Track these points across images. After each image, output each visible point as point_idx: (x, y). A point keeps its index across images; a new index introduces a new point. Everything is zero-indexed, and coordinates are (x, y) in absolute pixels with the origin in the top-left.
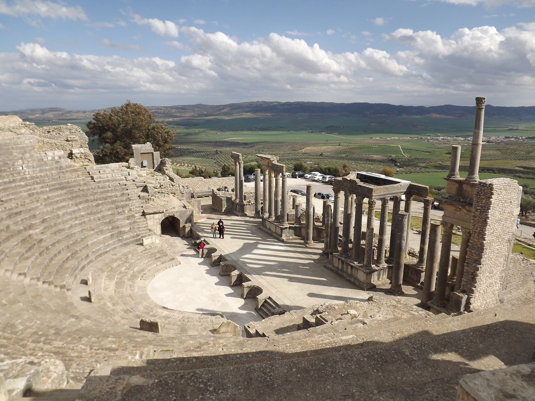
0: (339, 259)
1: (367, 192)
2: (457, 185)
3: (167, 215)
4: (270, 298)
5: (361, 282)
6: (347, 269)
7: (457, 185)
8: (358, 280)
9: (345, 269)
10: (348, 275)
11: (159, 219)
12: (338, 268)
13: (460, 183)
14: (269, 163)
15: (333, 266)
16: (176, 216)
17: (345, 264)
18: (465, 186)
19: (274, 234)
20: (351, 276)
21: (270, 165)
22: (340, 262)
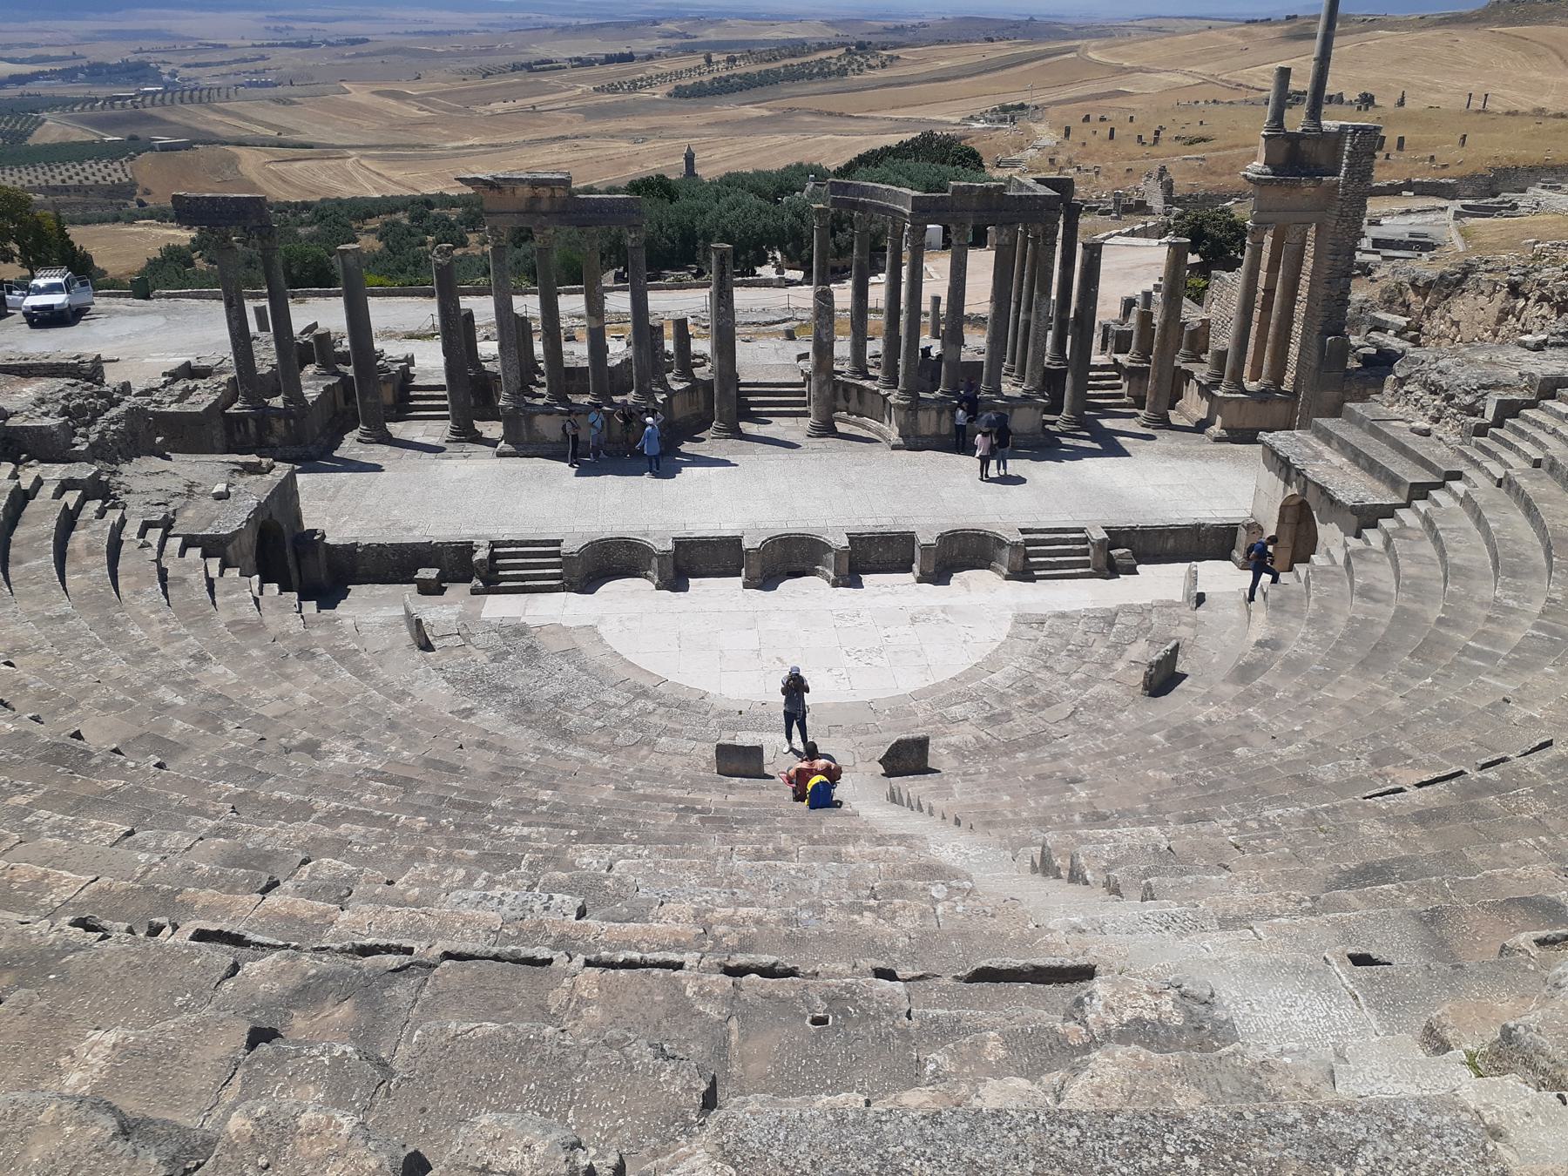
2: (1288, 145)
7: (1288, 145)
12: (938, 435)
13: (1294, 139)
14: (535, 199)
18: (1303, 145)
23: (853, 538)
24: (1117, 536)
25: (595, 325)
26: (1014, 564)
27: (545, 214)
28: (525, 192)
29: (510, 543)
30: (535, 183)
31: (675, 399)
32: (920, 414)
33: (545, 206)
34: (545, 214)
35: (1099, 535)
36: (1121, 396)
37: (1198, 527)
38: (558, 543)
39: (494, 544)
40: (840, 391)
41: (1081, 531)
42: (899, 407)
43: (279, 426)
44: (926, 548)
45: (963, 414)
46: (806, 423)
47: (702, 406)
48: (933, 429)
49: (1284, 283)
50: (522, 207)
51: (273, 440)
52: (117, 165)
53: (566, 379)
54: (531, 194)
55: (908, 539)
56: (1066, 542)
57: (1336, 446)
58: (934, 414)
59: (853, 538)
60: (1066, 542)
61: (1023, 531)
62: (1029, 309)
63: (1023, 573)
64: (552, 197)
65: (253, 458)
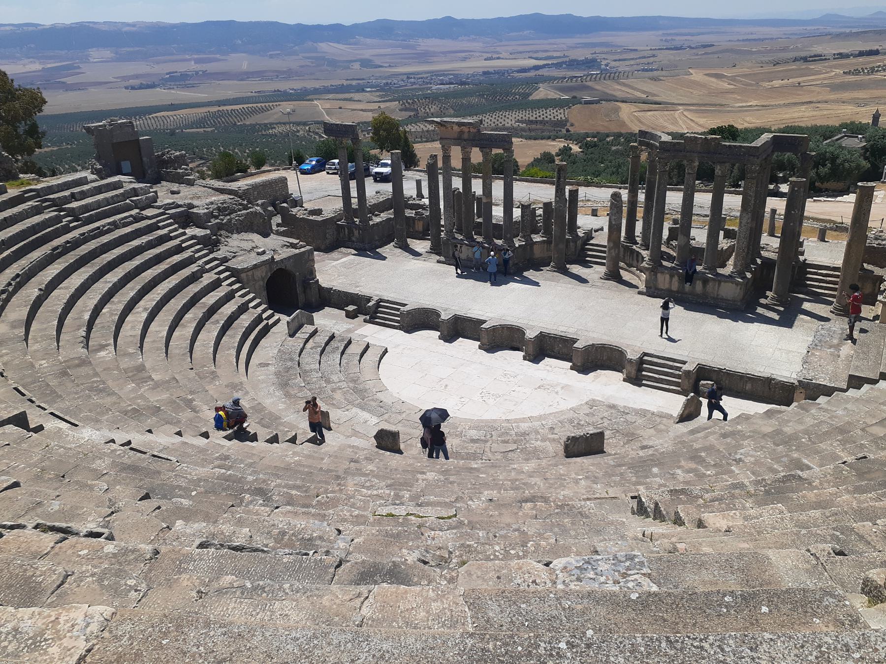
3: (275, 268)
4: (645, 354)
11: (263, 279)
14: (462, 132)
15: (657, 289)
16: (289, 266)
24: (703, 372)
27: (465, 140)
29: (388, 301)
30: (460, 124)
32: (659, 275)
33: (466, 136)
34: (465, 140)
39: (381, 300)
43: (356, 233)
45: (687, 283)
48: (667, 286)
50: (456, 136)
51: (354, 239)
52: (562, 111)
56: (671, 367)
58: (668, 276)
60: (671, 367)
63: (636, 379)
65: (295, 241)
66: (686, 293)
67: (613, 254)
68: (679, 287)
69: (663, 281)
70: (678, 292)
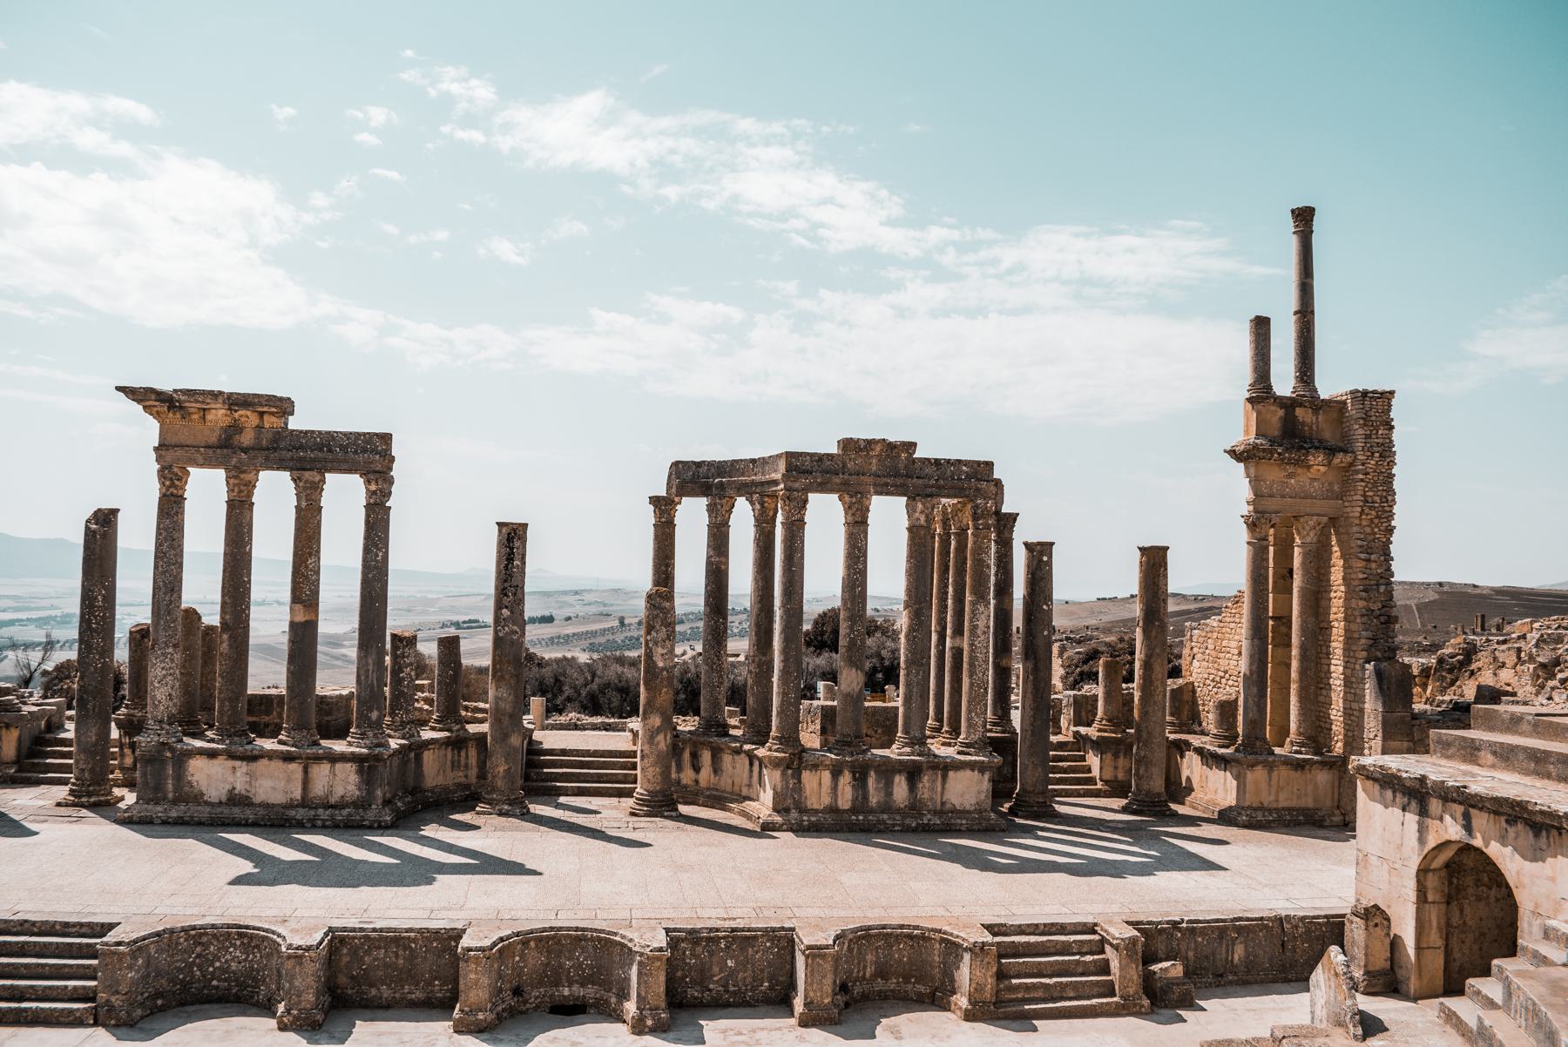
0: (836, 773)
1: (969, 477)
2: (1281, 413)
5: (968, 812)
6: (889, 794)
7: (1281, 413)
8: (954, 811)
9: (874, 800)
10: (899, 811)
12: (833, 809)
13: (1288, 405)
15: (803, 810)
17: (872, 781)
18: (1299, 412)
19: (300, 814)
20: (915, 807)
21: (247, 438)
22: (846, 779)
23: (674, 943)
24: (1153, 940)
25: (300, 618)
26: (978, 988)
27: (245, 450)
28: (218, 415)
31: (428, 756)
32: (806, 775)
33: (247, 438)
34: (245, 450)
35: (1120, 932)
36: (1092, 781)
37: (1280, 920)
38: (107, 928)
40: (687, 755)
41: (1091, 929)
42: (776, 763)
44: (815, 952)
46: (629, 802)
47: (473, 772)
48: (826, 800)
49: (1302, 604)
50: (213, 439)
53: (262, 714)
54: (228, 421)
55: (783, 940)
57: (1490, 759)
58: (826, 776)
59: (677, 939)
60: (1065, 949)
61: (992, 929)
62: (958, 631)
64: (259, 427)
66: (872, 811)
67: (662, 746)
68: (855, 800)
69: (817, 788)
70: (854, 810)
